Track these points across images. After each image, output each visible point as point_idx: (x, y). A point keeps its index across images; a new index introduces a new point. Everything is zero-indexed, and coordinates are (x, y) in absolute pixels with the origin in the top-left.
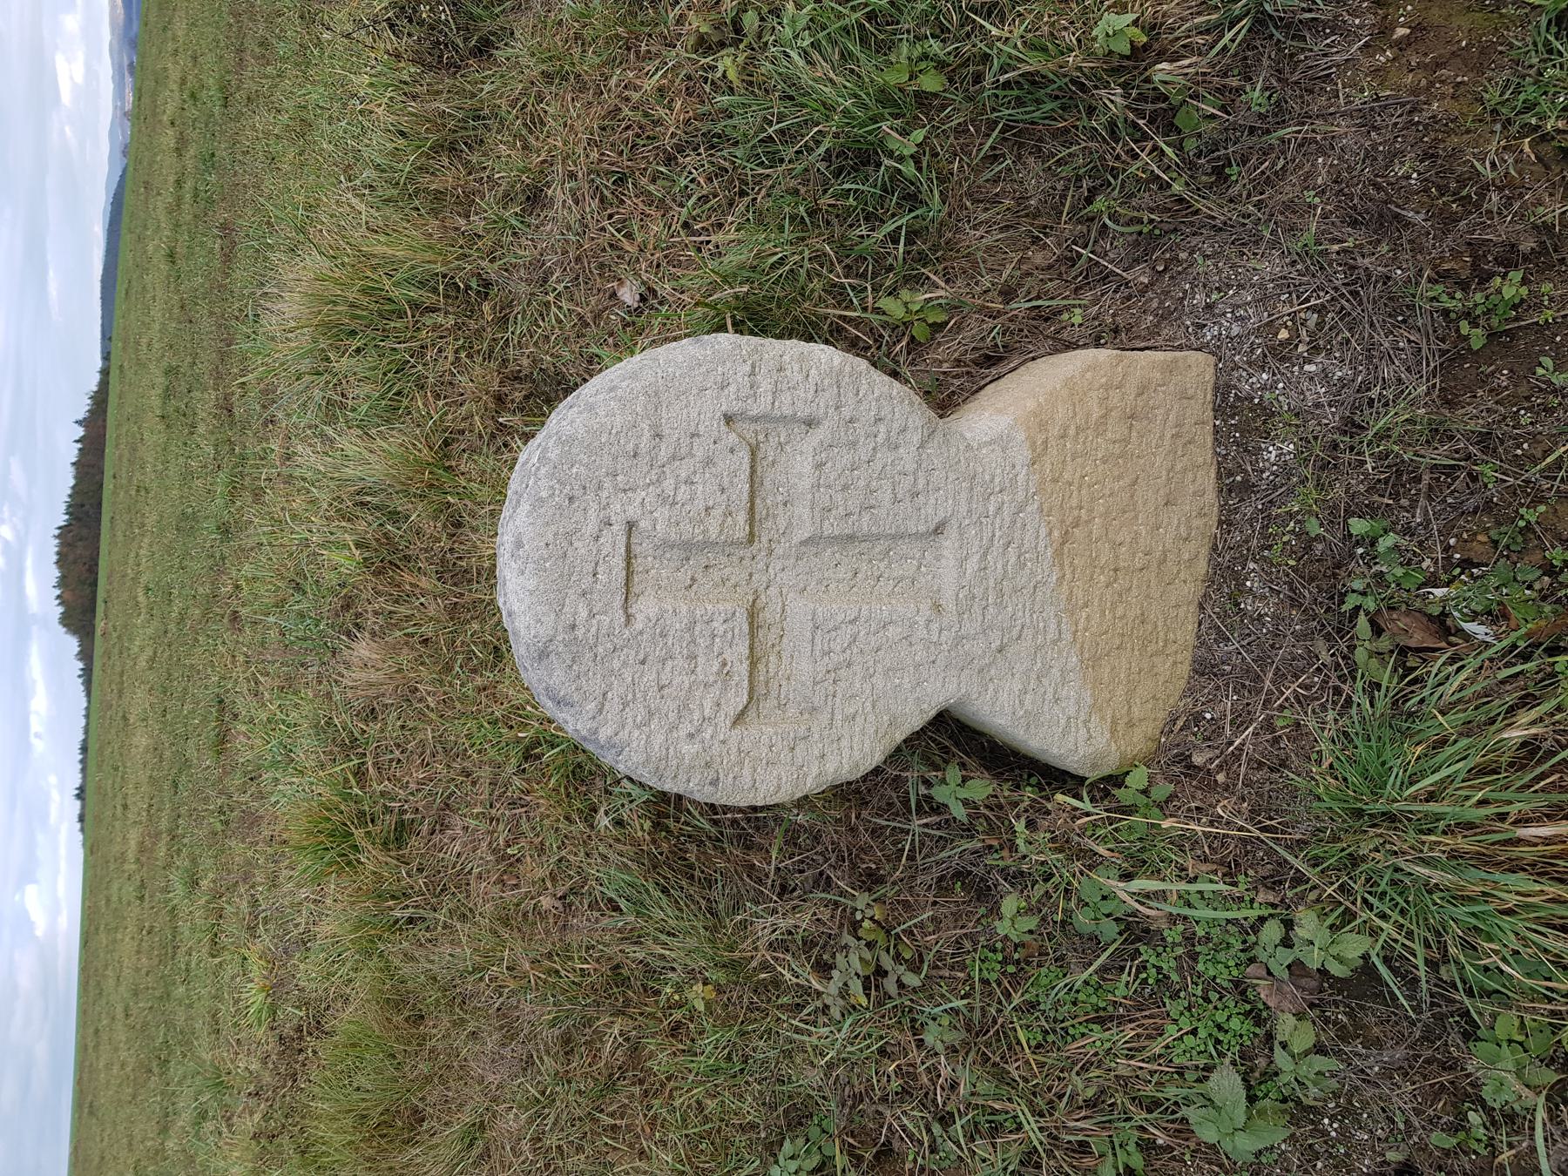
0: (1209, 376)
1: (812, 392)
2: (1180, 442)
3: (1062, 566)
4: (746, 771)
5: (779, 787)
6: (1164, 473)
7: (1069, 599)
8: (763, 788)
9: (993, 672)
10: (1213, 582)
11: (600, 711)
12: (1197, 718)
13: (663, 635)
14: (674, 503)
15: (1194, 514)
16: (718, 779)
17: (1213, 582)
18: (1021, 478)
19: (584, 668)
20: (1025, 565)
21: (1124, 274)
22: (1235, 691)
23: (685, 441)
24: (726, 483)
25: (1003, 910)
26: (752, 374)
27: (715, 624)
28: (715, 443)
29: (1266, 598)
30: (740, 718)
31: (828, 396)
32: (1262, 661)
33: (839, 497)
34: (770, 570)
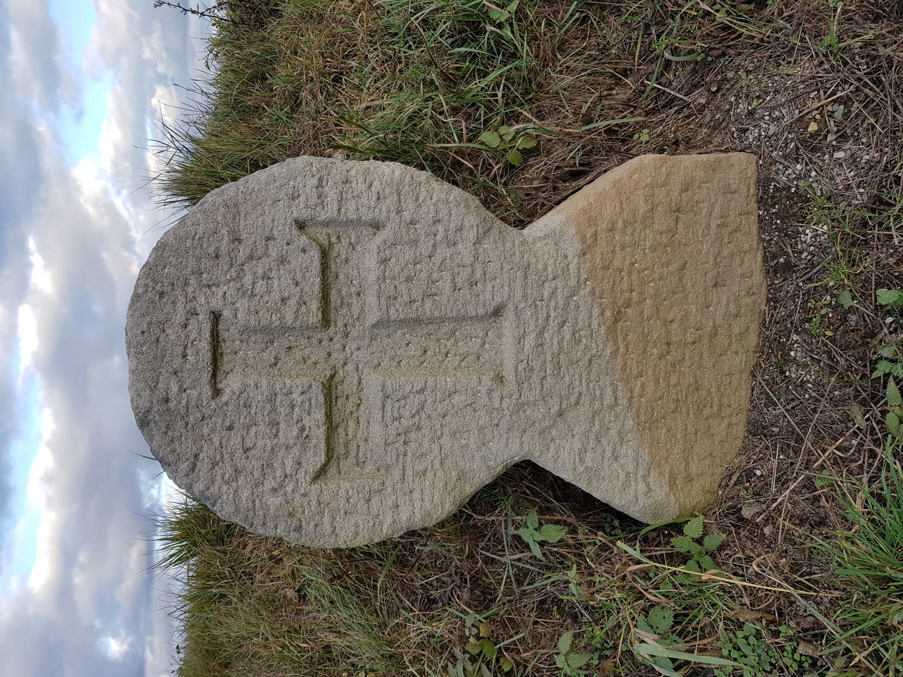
0: (752, 171)
1: (374, 199)
2: (726, 231)
3: (615, 342)
4: (327, 520)
5: (357, 533)
6: (711, 258)
7: (624, 369)
8: (342, 534)
9: (554, 433)
10: (763, 353)
11: (193, 469)
12: (749, 474)
13: (247, 406)
14: (253, 295)
15: (743, 293)
16: (301, 526)
17: (763, 353)
18: (572, 267)
19: (177, 434)
20: (580, 340)
21: (685, 98)
22: (782, 451)
23: (261, 244)
24: (299, 277)
25: (560, 645)
26: (320, 185)
27: (294, 396)
28: (288, 244)
29: (808, 365)
30: (320, 474)
31: (390, 202)
32: (804, 423)
33: (403, 287)
34: (347, 349)
